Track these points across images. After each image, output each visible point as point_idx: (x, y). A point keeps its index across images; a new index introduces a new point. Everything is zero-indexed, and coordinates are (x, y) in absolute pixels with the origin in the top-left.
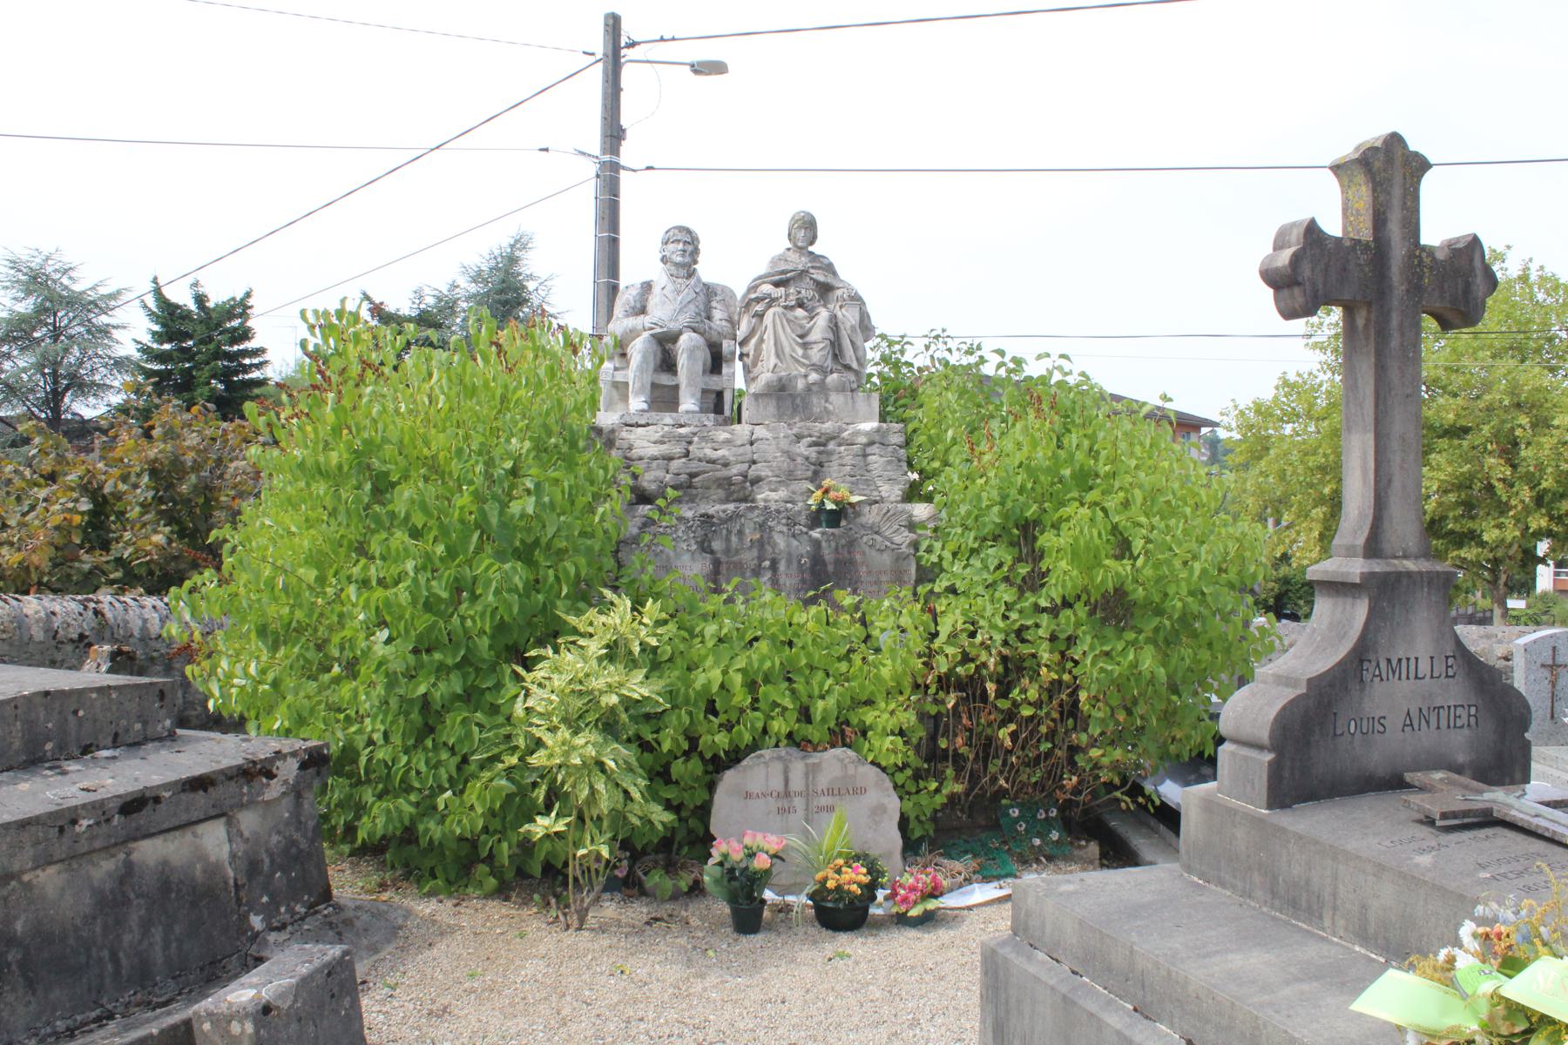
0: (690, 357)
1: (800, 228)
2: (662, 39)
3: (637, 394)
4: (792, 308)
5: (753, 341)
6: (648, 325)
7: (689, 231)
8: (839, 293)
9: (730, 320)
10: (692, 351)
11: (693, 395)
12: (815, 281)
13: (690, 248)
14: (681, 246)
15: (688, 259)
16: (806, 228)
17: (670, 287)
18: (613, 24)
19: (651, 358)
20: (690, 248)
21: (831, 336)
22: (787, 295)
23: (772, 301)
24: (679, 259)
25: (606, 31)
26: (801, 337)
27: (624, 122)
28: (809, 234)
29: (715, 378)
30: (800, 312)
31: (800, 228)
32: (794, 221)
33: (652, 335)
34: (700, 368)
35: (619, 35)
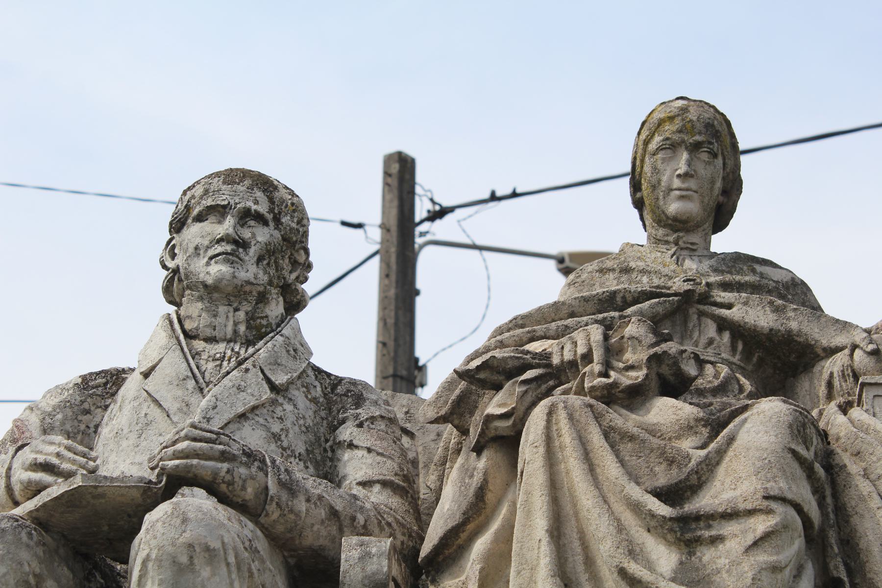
1: (671, 146)
2: (494, 198)
4: (634, 397)
5: (481, 545)
6: (21, 475)
8: (834, 365)
10: (182, 567)
12: (740, 333)
13: (262, 235)
14: (227, 226)
15: (250, 271)
16: (695, 160)
17: (174, 365)
18: (401, 173)
20: (262, 235)
21: (804, 493)
22: (612, 352)
23: (555, 376)
24: (217, 270)
25: (386, 184)
26: (670, 495)
28: (710, 170)
30: (665, 411)
31: (671, 146)
32: (650, 127)
33: (41, 520)
35: (412, 193)
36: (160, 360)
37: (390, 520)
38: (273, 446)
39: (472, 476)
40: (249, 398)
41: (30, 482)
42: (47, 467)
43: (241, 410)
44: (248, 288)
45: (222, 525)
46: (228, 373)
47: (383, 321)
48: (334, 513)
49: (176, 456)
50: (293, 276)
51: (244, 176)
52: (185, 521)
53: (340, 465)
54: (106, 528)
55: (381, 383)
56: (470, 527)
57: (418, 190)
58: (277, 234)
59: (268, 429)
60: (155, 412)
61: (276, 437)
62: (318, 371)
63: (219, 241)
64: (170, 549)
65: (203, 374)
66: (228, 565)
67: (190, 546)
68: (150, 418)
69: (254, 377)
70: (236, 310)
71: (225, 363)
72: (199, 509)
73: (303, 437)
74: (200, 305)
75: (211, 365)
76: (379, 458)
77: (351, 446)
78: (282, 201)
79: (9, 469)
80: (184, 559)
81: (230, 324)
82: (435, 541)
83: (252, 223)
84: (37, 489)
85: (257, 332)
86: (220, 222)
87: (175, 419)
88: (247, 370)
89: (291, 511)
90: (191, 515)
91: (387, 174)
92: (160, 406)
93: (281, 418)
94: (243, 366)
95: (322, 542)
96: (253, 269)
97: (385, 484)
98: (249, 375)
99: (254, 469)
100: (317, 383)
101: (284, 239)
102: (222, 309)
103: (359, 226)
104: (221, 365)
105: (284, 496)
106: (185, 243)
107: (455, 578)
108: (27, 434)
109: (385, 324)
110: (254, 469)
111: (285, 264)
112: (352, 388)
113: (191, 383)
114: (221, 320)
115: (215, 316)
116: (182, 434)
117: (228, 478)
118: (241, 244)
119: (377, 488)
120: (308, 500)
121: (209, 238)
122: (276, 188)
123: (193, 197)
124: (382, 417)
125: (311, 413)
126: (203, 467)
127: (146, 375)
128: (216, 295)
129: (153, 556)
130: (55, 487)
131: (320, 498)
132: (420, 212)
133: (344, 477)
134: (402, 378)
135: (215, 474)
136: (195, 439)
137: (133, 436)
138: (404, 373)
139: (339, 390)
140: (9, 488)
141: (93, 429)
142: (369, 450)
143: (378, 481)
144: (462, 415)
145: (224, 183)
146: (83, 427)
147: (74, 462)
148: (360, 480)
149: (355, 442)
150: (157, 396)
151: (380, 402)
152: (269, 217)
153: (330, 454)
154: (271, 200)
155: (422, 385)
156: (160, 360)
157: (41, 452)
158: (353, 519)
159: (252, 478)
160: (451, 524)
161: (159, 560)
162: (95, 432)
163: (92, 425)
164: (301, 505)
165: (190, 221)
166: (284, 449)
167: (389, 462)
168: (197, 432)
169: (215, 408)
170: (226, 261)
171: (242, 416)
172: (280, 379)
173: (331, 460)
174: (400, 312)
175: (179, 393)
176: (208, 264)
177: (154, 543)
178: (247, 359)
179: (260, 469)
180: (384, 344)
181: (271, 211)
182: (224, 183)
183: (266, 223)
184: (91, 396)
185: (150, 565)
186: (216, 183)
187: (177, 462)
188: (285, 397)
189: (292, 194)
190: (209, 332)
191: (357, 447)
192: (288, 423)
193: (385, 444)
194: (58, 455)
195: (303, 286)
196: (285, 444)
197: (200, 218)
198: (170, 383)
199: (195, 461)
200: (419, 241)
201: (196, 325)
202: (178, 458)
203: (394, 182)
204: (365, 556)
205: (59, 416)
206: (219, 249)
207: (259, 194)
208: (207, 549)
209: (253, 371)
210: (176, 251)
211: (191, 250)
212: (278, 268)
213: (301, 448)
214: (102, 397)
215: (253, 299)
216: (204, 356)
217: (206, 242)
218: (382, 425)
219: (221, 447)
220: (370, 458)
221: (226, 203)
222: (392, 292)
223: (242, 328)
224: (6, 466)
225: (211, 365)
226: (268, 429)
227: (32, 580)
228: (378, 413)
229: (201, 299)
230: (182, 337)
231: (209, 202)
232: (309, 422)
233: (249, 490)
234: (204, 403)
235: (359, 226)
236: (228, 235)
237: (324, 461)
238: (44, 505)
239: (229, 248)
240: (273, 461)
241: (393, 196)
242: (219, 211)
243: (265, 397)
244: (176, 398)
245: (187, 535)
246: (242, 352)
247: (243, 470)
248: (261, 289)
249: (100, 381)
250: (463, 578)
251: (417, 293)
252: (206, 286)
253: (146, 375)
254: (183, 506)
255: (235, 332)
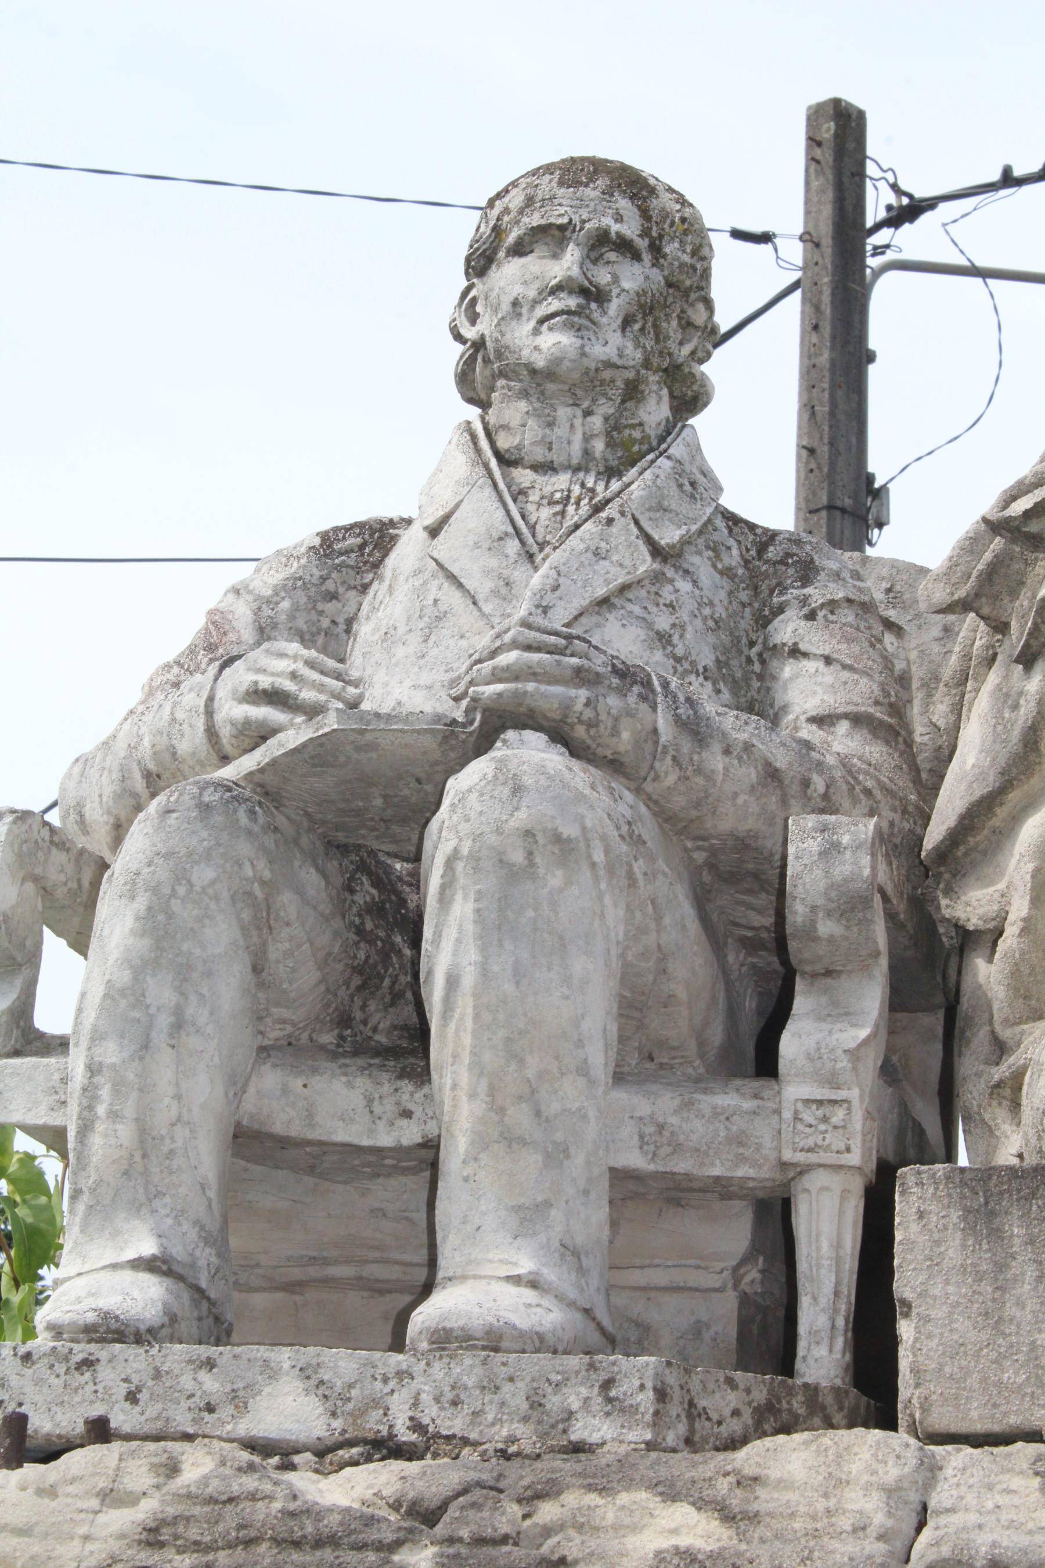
0: (496, 926)
2: (1009, 180)
3: (101, 1213)
6: (233, 711)
7: (633, 184)
9: (889, 724)
10: (514, 870)
11: (528, 1218)
13: (631, 278)
14: (568, 263)
15: (611, 343)
17: (482, 513)
18: (839, 139)
19: (221, 936)
20: (631, 278)
24: (552, 343)
25: (812, 160)
27: (879, 464)
29: (732, 1099)
33: (267, 790)
34: (584, 1007)
35: (860, 175)
36: (457, 506)
37: (869, 784)
38: (658, 656)
39: (1016, 707)
40: (614, 570)
41: (247, 723)
42: (275, 697)
43: (601, 592)
44: (607, 374)
45: (580, 798)
46: (577, 527)
47: (809, 409)
48: (772, 775)
49: (496, 676)
50: (686, 350)
51: (596, 171)
52: (517, 790)
53: (777, 686)
54: (378, 802)
55: (806, 520)
56: (1014, 797)
57: (871, 169)
58: (657, 276)
59: (649, 625)
60: (452, 597)
61: (663, 639)
62: (733, 520)
63: (555, 290)
64: (493, 839)
65: (532, 528)
66: (593, 865)
67: (528, 834)
68: (443, 607)
69: (623, 533)
70: (588, 413)
71: (571, 509)
72: (541, 770)
73: (711, 638)
74: (523, 405)
75: (545, 513)
76: (846, 675)
77: (796, 652)
78: (665, 215)
79: (211, 699)
80: (518, 857)
81: (578, 438)
82: (951, 821)
83: (612, 256)
84: (259, 735)
85: (625, 453)
86: (555, 256)
87: (487, 608)
88: (610, 521)
89: (699, 771)
90: (528, 781)
91: (813, 141)
92: (460, 586)
93: (670, 606)
94: (603, 515)
95: (750, 824)
96: (616, 339)
97: (857, 720)
98: (614, 529)
99: (632, 699)
100: (731, 542)
101: (670, 285)
102: (563, 413)
103: (765, 238)
104: (563, 513)
105: (686, 746)
106: (494, 294)
107: (988, 886)
108: (232, 636)
109: (813, 414)
110: (632, 699)
111: (672, 327)
112: (795, 549)
113: (513, 546)
114: (561, 431)
115: (551, 425)
116: (507, 638)
117: (588, 714)
118: (592, 295)
119: (843, 727)
120: (727, 752)
121: (536, 285)
122: (652, 191)
123: (506, 211)
124: (849, 601)
125: (722, 595)
126: (544, 696)
127: (434, 531)
128: (551, 387)
129: (465, 851)
130: (291, 732)
131: (748, 747)
132: (874, 210)
133: (785, 708)
134: (843, 511)
135: (567, 707)
136: (528, 648)
137: (414, 641)
138: (848, 502)
139: (772, 553)
140: (211, 733)
141: (342, 627)
142: (828, 660)
143: (846, 716)
144: (995, 598)
145: (561, 183)
146: (325, 623)
147: (321, 688)
148: (814, 713)
149: (802, 647)
150: (454, 569)
151: (846, 574)
152: (642, 244)
153: (757, 667)
154: (645, 214)
155: (880, 525)
156: (457, 506)
157: (263, 671)
158: (806, 783)
159: (630, 713)
160: (979, 792)
161: (474, 858)
162: (348, 631)
163: (341, 620)
164: (715, 761)
165: (501, 254)
166: (678, 660)
167: (864, 681)
168: (533, 634)
169: (556, 588)
170: (568, 326)
171: (604, 603)
172: (669, 535)
173: (761, 677)
174: (840, 393)
175: (493, 562)
176: (536, 332)
177: (464, 828)
178: (608, 501)
179: (643, 698)
180: (811, 451)
181: (645, 233)
182: (561, 183)
183: (636, 256)
184: (338, 568)
185: (460, 866)
186: (547, 184)
187: (499, 687)
188: (676, 568)
189: (682, 201)
190: (540, 454)
191: (805, 655)
192: (684, 615)
193: (856, 649)
194: (294, 676)
195: (705, 368)
196: (680, 651)
197: (519, 250)
198: (477, 545)
199: (531, 686)
200: (873, 262)
201: (516, 442)
202: (500, 681)
203: (826, 155)
204: (831, 850)
205: (286, 605)
206: (554, 304)
207: (623, 203)
208: (557, 838)
209: (620, 522)
210: (479, 308)
211: (505, 307)
212: (659, 336)
213: (706, 658)
214: (358, 570)
215: (616, 394)
216: (534, 497)
217: (532, 293)
218: (848, 616)
219: (574, 661)
220: (829, 675)
221: (565, 220)
222: (824, 358)
223: (599, 446)
224: (205, 695)
225: (545, 513)
226: (649, 625)
227: (258, 892)
228: (840, 595)
229: (525, 394)
230: (493, 463)
231: (535, 219)
232: (720, 611)
233: (625, 735)
234: (537, 580)
235: (765, 238)
236: (570, 279)
237: (747, 680)
238: (274, 763)
239: (572, 302)
240: (665, 685)
241: (825, 182)
242: (552, 236)
243: (642, 569)
244: (487, 572)
245: (522, 814)
246: (600, 487)
247: (613, 702)
248: (631, 375)
249: (353, 541)
250: (1001, 886)
251: (871, 357)
252: (533, 372)
253: (434, 531)
254: (512, 765)
255: (587, 453)
